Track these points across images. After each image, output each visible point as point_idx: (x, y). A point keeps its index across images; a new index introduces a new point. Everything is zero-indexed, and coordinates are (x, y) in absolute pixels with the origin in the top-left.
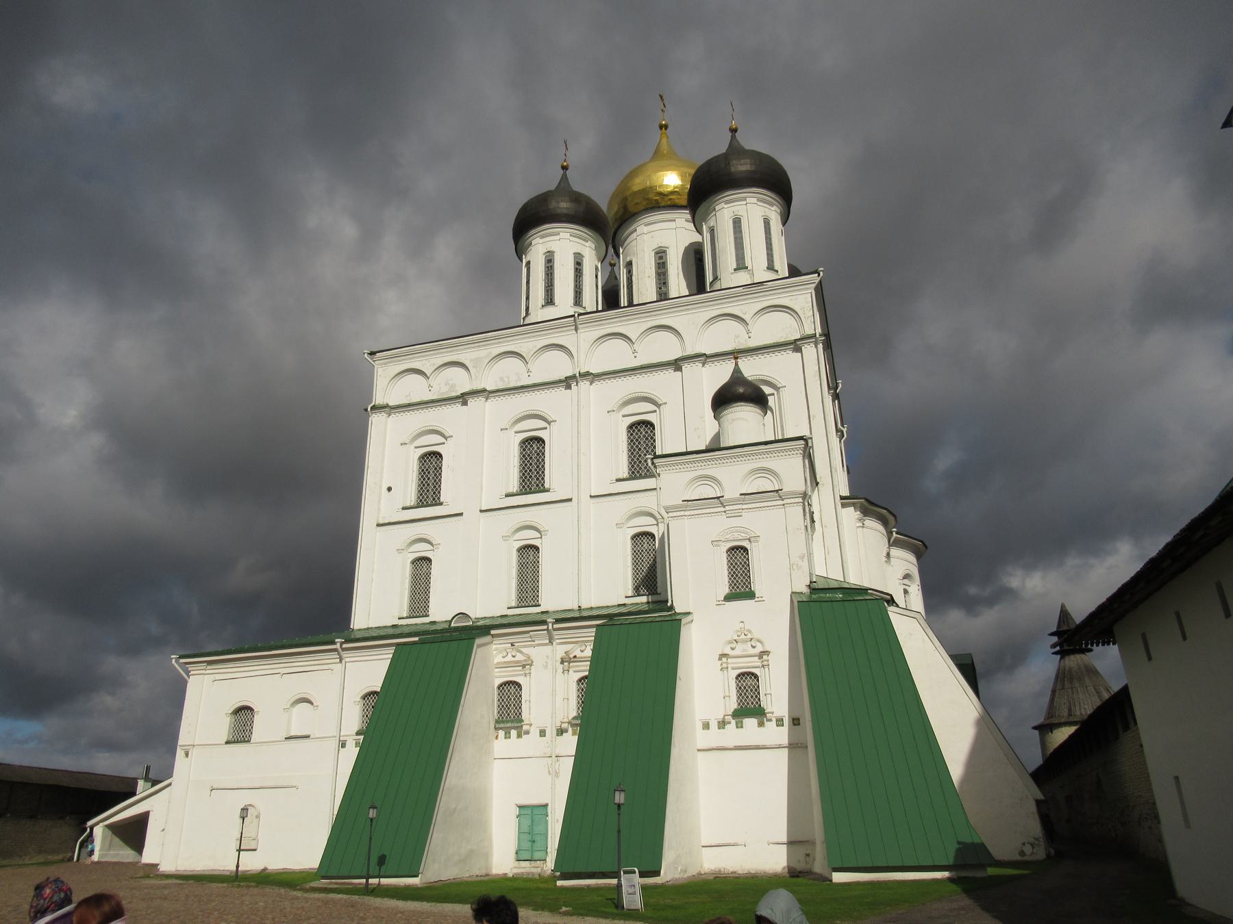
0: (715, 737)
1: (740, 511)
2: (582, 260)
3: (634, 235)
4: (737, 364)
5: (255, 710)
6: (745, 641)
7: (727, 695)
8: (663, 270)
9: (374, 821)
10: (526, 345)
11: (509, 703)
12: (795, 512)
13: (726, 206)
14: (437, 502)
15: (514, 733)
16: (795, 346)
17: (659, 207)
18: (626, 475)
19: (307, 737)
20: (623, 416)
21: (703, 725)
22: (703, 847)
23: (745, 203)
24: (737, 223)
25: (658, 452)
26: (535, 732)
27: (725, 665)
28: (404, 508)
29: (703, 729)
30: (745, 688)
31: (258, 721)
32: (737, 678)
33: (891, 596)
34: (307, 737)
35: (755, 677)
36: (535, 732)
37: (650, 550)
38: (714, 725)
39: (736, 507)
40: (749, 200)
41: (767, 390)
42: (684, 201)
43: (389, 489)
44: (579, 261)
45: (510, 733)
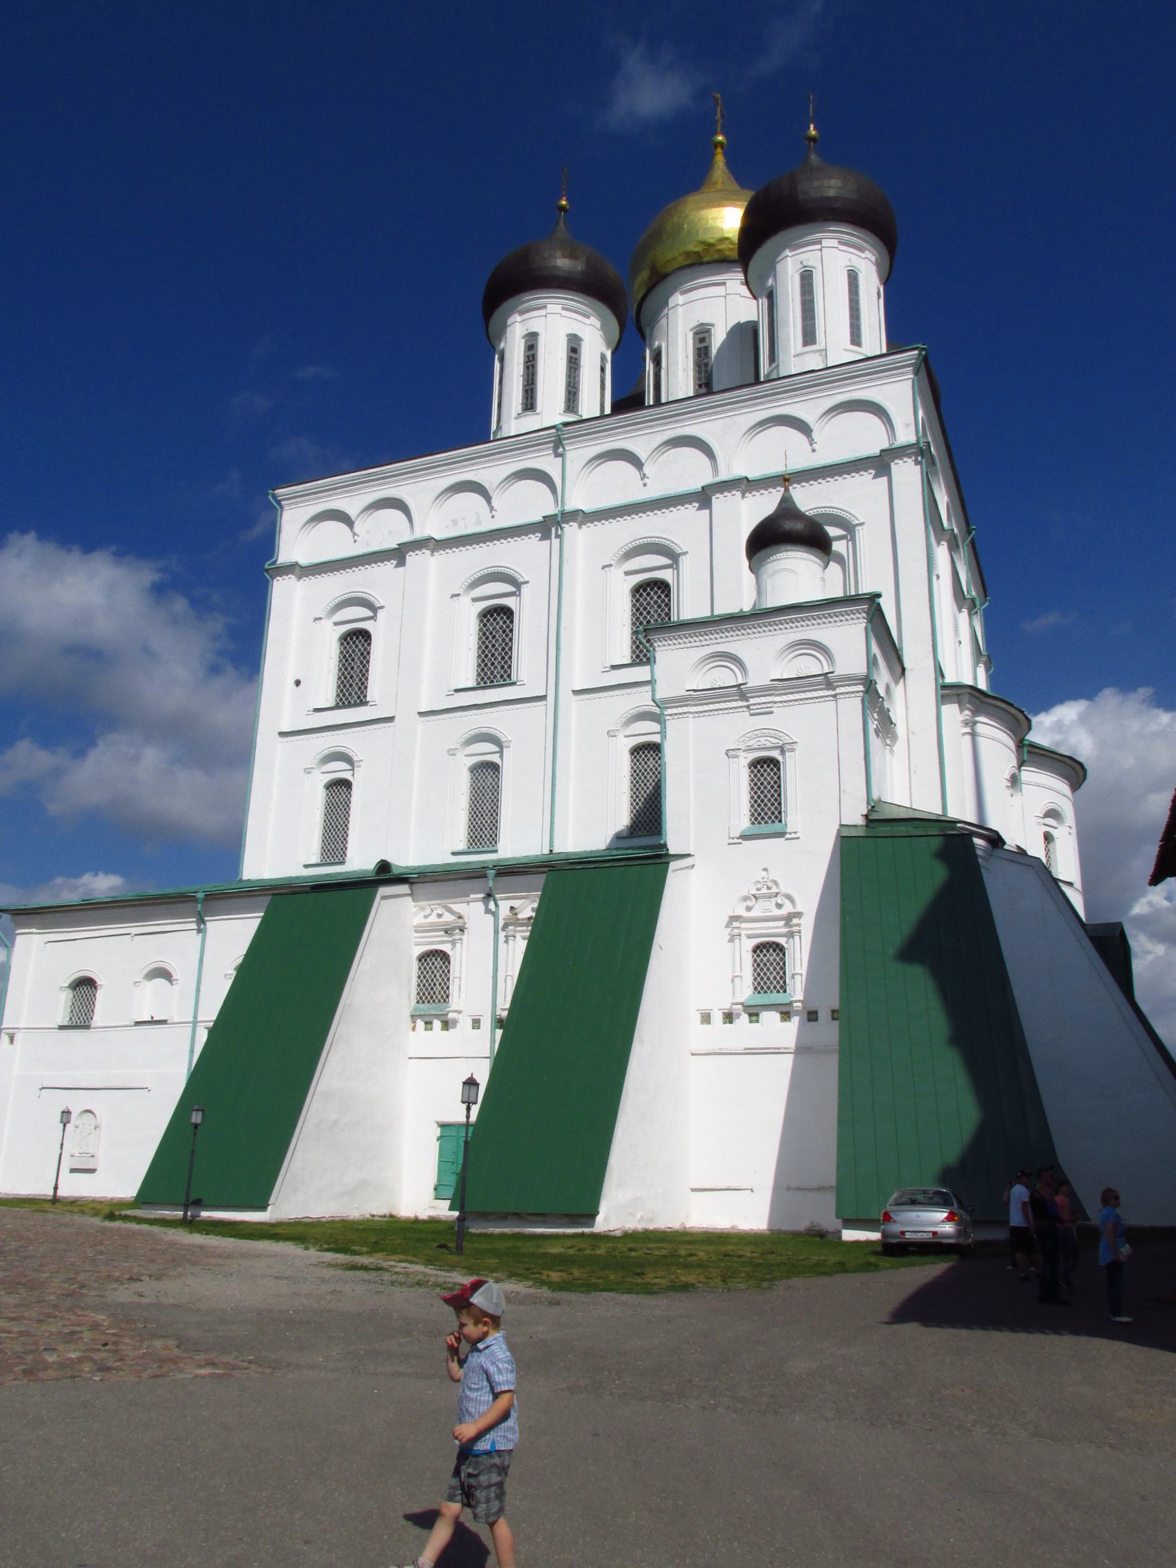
0: (720, 1034)
1: (769, 705)
2: (580, 345)
4: (787, 490)
5: (99, 983)
6: (769, 897)
7: (738, 974)
9: (199, 1127)
10: (490, 473)
12: (851, 707)
14: (362, 702)
15: (437, 1024)
16: (880, 464)
17: (701, 264)
18: (628, 661)
19: (164, 1022)
21: (702, 1017)
22: (693, 1190)
23: (818, 247)
24: (807, 279)
26: (465, 1023)
27: (736, 931)
28: (317, 710)
29: (702, 1023)
30: (765, 965)
31: (101, 997)
32: (754, 951)
33: (996, 832)
34: (164, 1022)
36: (465, 1023)
38: (717, 1017)
39: (764, 699)
41: (832, 531)
42: (734, 254)
43: (298, 683)
44: (574, 346)
45: (431, 1023)
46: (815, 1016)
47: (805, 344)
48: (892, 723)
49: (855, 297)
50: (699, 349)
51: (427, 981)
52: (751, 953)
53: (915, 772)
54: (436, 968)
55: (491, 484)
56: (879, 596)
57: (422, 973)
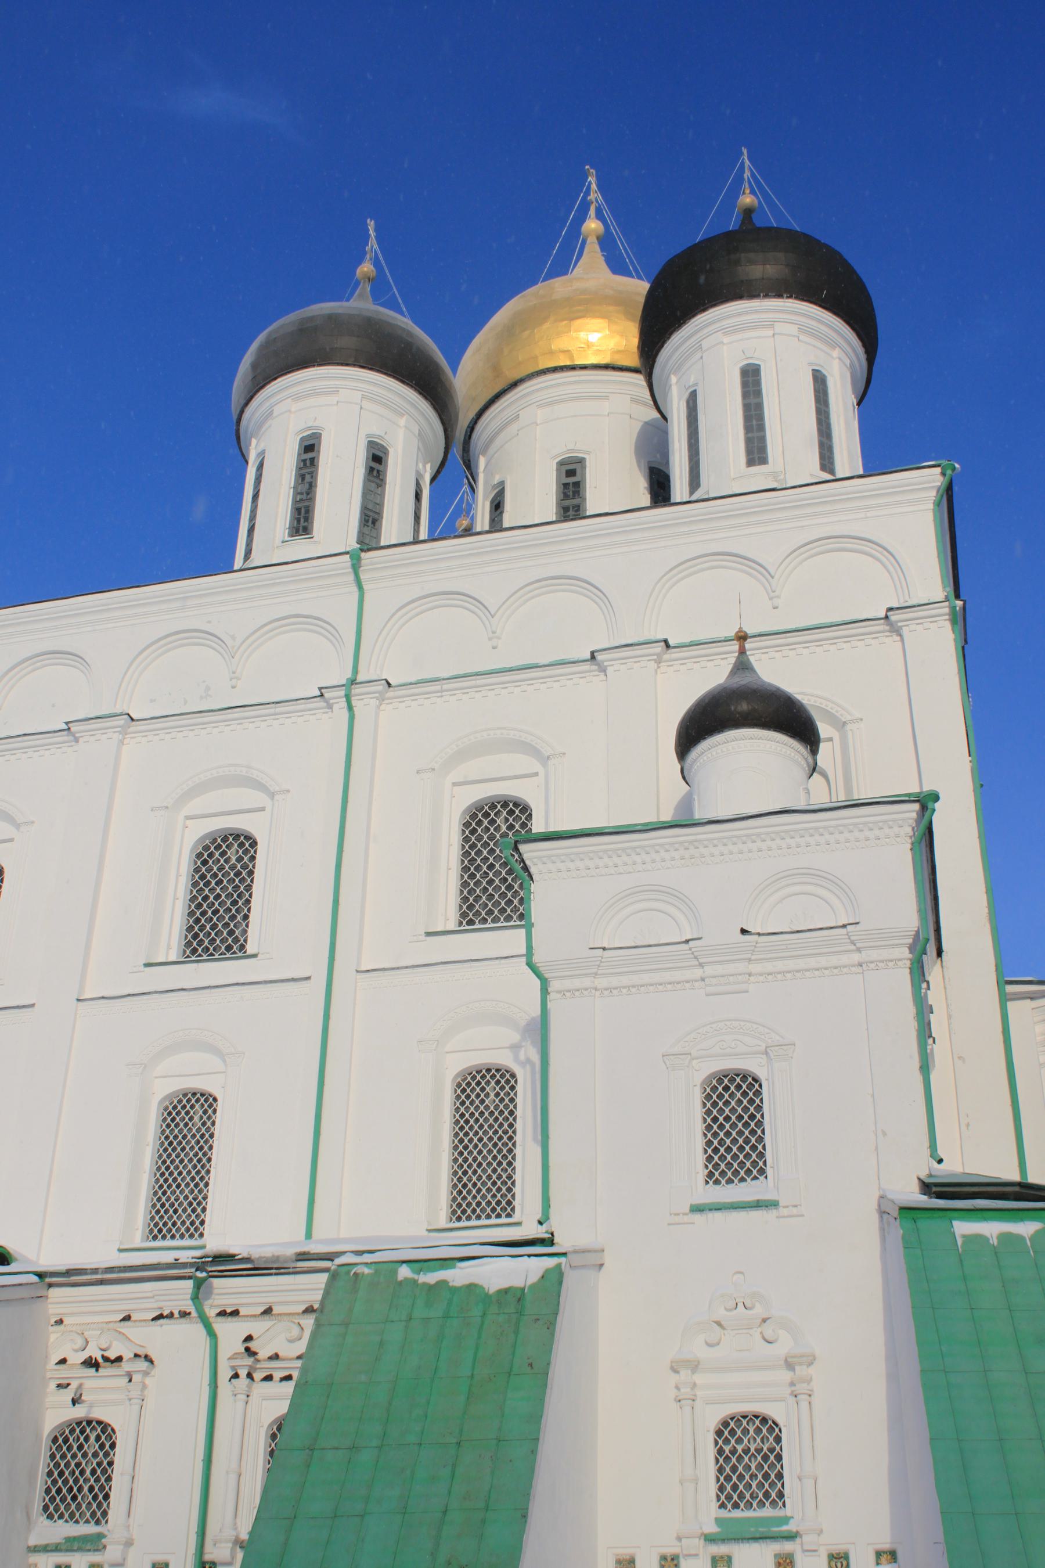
3: (513, 428)
4: (742, 651)
8: (575, 501)
11: (76, 1481)
13: (726, 340)
20: (454, 784)
23: (771, 333)
24: (751, 377)
25: (538, 826)
27: (685, 1391)
32: (719, 1433)
35: (771, 1430)
37: (501, 1112)
39: (730, 968)
40: (779, 328)
46: (845, 1563)
47: (750, 463)
48: (930, 1036)
49: (823, 408)
50: (566, 486)
51: (65, 1482)
52: (711, 1436)
53: (968, 1125)
54: (85, 1455)
55: (233, 638)
56: (936, 798)
57: (57, 1465)
